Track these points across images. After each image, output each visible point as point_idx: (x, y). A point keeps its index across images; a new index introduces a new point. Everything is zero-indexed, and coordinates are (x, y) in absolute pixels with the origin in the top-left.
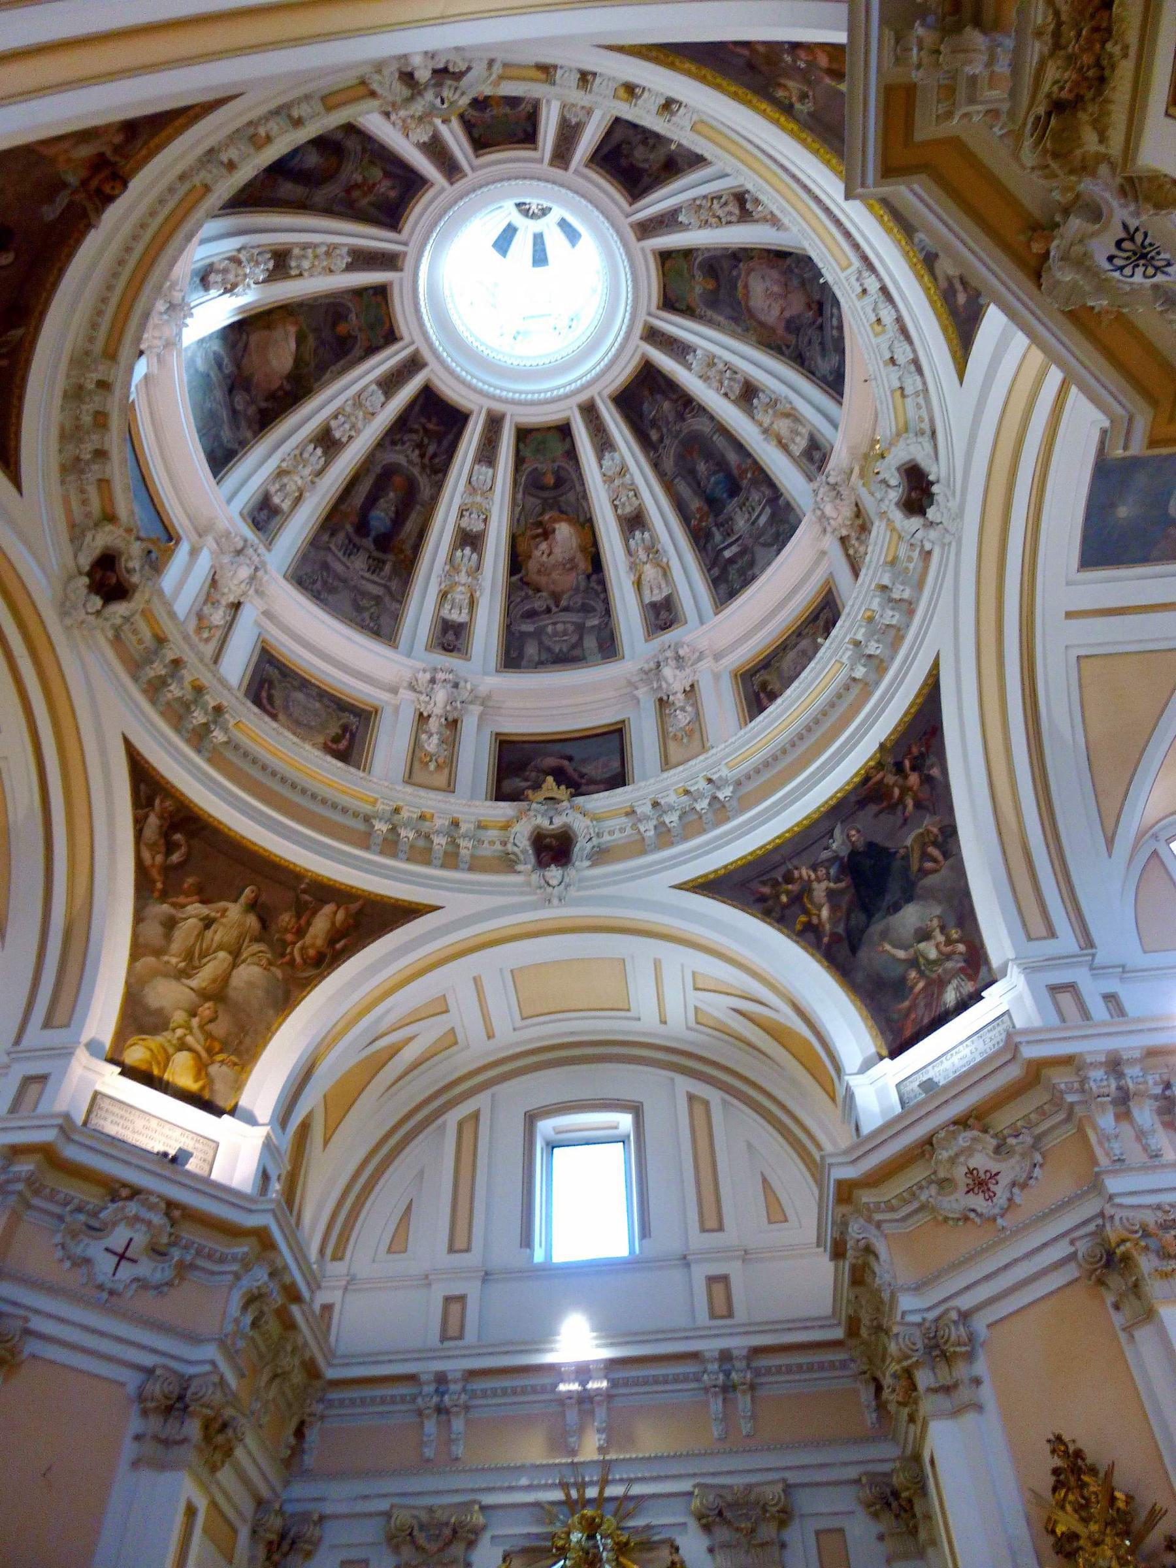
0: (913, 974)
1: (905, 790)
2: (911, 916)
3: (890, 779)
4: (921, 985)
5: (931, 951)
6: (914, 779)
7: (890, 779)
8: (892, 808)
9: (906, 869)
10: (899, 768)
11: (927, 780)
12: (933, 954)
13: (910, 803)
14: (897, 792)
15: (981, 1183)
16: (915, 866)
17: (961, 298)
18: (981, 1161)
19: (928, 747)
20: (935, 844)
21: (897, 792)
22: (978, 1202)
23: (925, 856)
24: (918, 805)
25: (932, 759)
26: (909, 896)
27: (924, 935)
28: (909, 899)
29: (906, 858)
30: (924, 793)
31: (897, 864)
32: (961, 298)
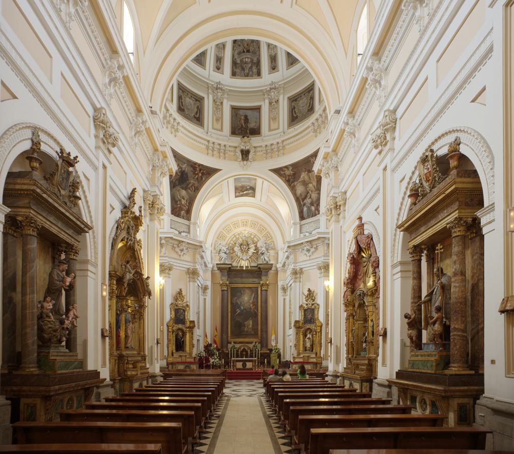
0: (179, 202)
1: (198, 174)
2: (184, 192)
3: (198, 169)
4: (179, 206)
5: (183, 202)
6: (200, 174)
7: (198, 169)
8: (194, 174)
9: (188, 185)
10: (200, 170)
11: (202, 178)
12: (183, 203)
13: (197, 177)
14: (197, 172)
15: (182, 250)
16: (189, 186)
17: (282, 173)
18: (185, 248)
19: (207, 174)
20: (194, 187)
21: (197, 172)
22: (179, 252)
23: (192, 186)
24: (197, 178)
25: (205, 176)
26: (186, 189)
27: (184, 199)
28: (185, 190)
29: (190, 183)
30: (200, 179)
31: (188, 182)
32: (282, 173)
